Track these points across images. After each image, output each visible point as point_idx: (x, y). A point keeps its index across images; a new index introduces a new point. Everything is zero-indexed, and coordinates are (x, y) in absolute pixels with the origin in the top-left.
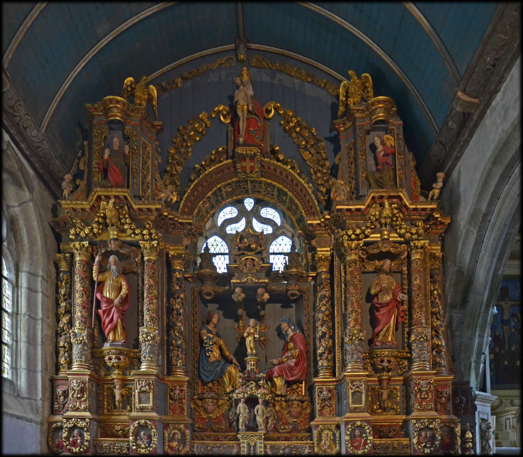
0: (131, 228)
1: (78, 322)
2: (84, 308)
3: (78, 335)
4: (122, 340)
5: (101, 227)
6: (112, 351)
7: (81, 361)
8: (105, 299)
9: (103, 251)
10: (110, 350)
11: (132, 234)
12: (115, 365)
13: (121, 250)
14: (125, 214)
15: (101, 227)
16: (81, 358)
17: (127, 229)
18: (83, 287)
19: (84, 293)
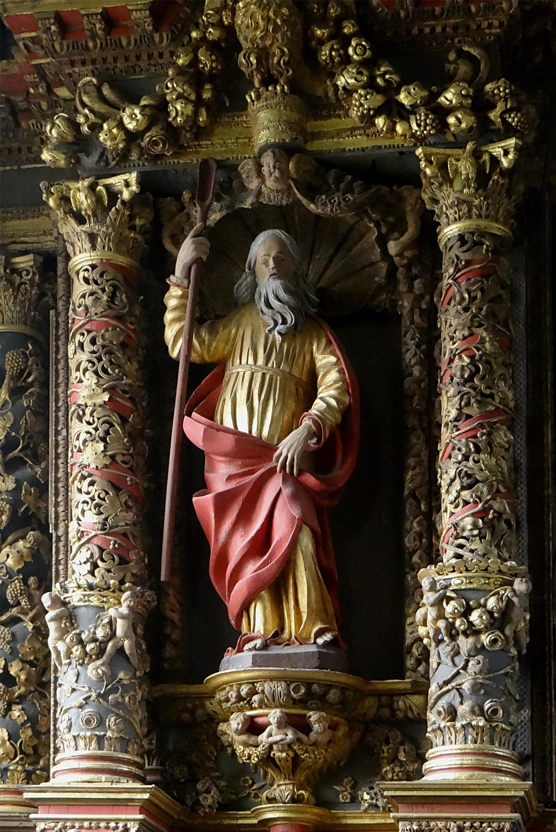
0: (371, 85)
1: (84, 555)
2: (117, 489)
3: (82, 613)
4: (320, 633)
5: (206, 95)
6: (267, 687)
7: (100, 740)
8: (228, 442)
9: (215, 217)
10: (252, 682)
11: (379, 112)
12: (277, 754)
13: (312, 200)
14: (339, 22)
15: (206, 95)
16: (101, 723)
17: (349, 91)
18: (111, 390)
19: (115, 419)
